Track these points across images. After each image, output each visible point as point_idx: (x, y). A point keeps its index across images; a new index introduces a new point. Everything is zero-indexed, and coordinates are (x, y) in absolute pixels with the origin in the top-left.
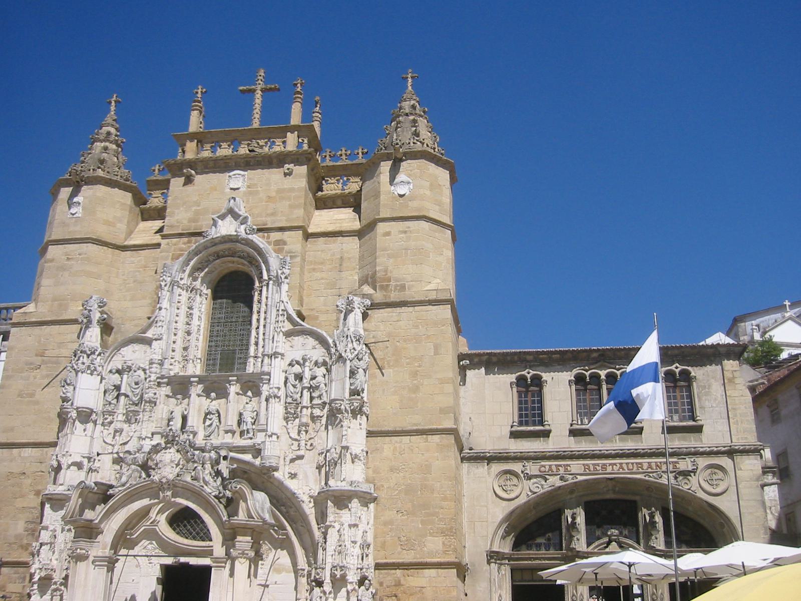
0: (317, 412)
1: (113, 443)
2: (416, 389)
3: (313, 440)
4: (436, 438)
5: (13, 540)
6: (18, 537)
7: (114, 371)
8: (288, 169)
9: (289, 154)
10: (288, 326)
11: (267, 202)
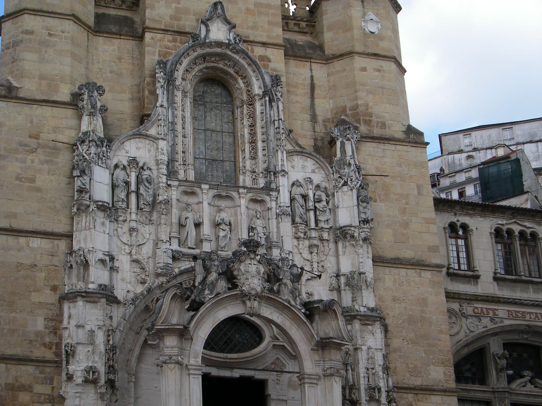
0: (325, 236)
1: (129, 243)
2: (406, 225)
3: (322, 263)
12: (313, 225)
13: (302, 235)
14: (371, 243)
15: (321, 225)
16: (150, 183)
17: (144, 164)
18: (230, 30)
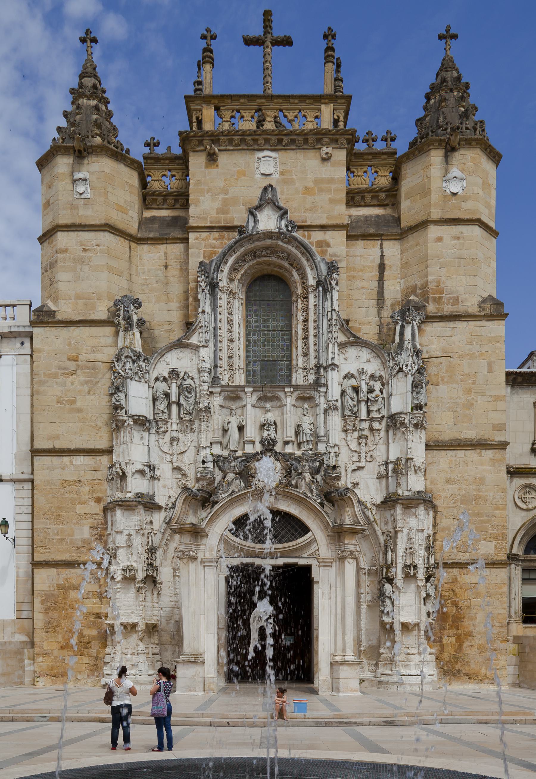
0: (376, 425)
1: (170, 452)
3: (371, 453)
4: (489, 453)
5: (80, 544)
6: (84, 541)
7: (162, 379)
8: (327, 153)
9: (327, 132)
10: (342, 338)
11: (304, 194)
12: (363, 415)
13: (351, 428)
14: (425, 429)
16: (190, 392)
17: (185, 373)
18: (282, 217)
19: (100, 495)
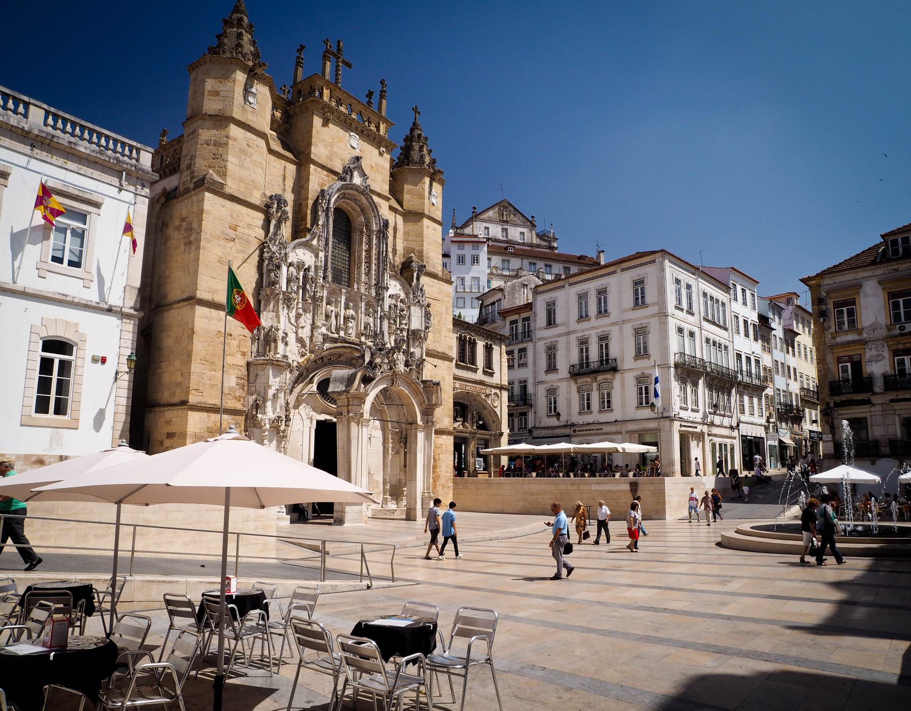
4: (446, 363)
15: (403, 326)
19: (245, 350)
